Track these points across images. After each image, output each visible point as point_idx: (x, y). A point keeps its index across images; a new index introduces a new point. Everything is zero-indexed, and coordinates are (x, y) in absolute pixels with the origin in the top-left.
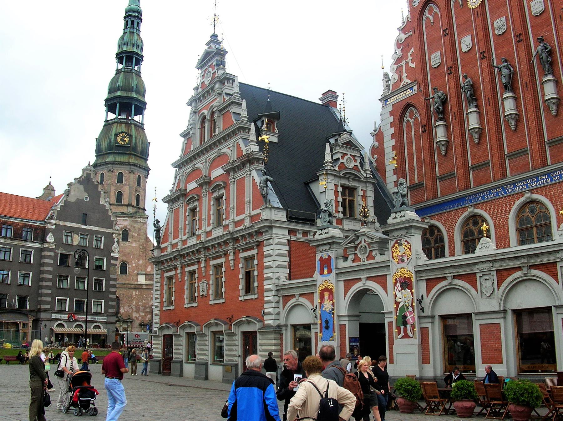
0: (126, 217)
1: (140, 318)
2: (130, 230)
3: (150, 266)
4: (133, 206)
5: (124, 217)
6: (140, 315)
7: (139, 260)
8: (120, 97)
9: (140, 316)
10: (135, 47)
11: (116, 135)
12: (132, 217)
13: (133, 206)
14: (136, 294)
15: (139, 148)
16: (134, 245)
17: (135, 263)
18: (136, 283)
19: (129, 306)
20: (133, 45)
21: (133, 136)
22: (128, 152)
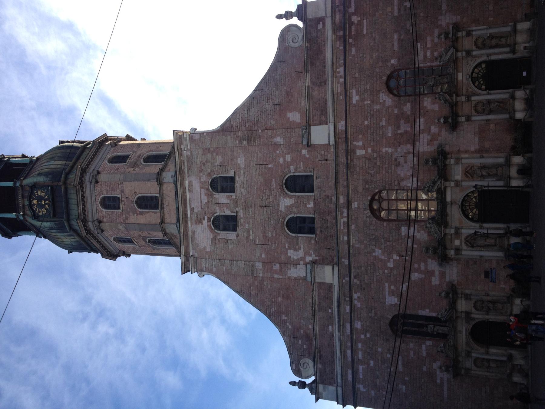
0: (182, 185)
1: (434, 129)
2: (209, 175)
3: (290, 115)
4: (162, 170)
5: (184, 189)
6: (423, 131)
7: (277, 146)
9: (427, 130)
11: (36, 217)
12: (182, 173)
13: (162, 170)
14: (364, 147)
16: (241, 161)
17: (283, 155)
18: (333, 149)
19: (398, 165)
21: (35, 180)
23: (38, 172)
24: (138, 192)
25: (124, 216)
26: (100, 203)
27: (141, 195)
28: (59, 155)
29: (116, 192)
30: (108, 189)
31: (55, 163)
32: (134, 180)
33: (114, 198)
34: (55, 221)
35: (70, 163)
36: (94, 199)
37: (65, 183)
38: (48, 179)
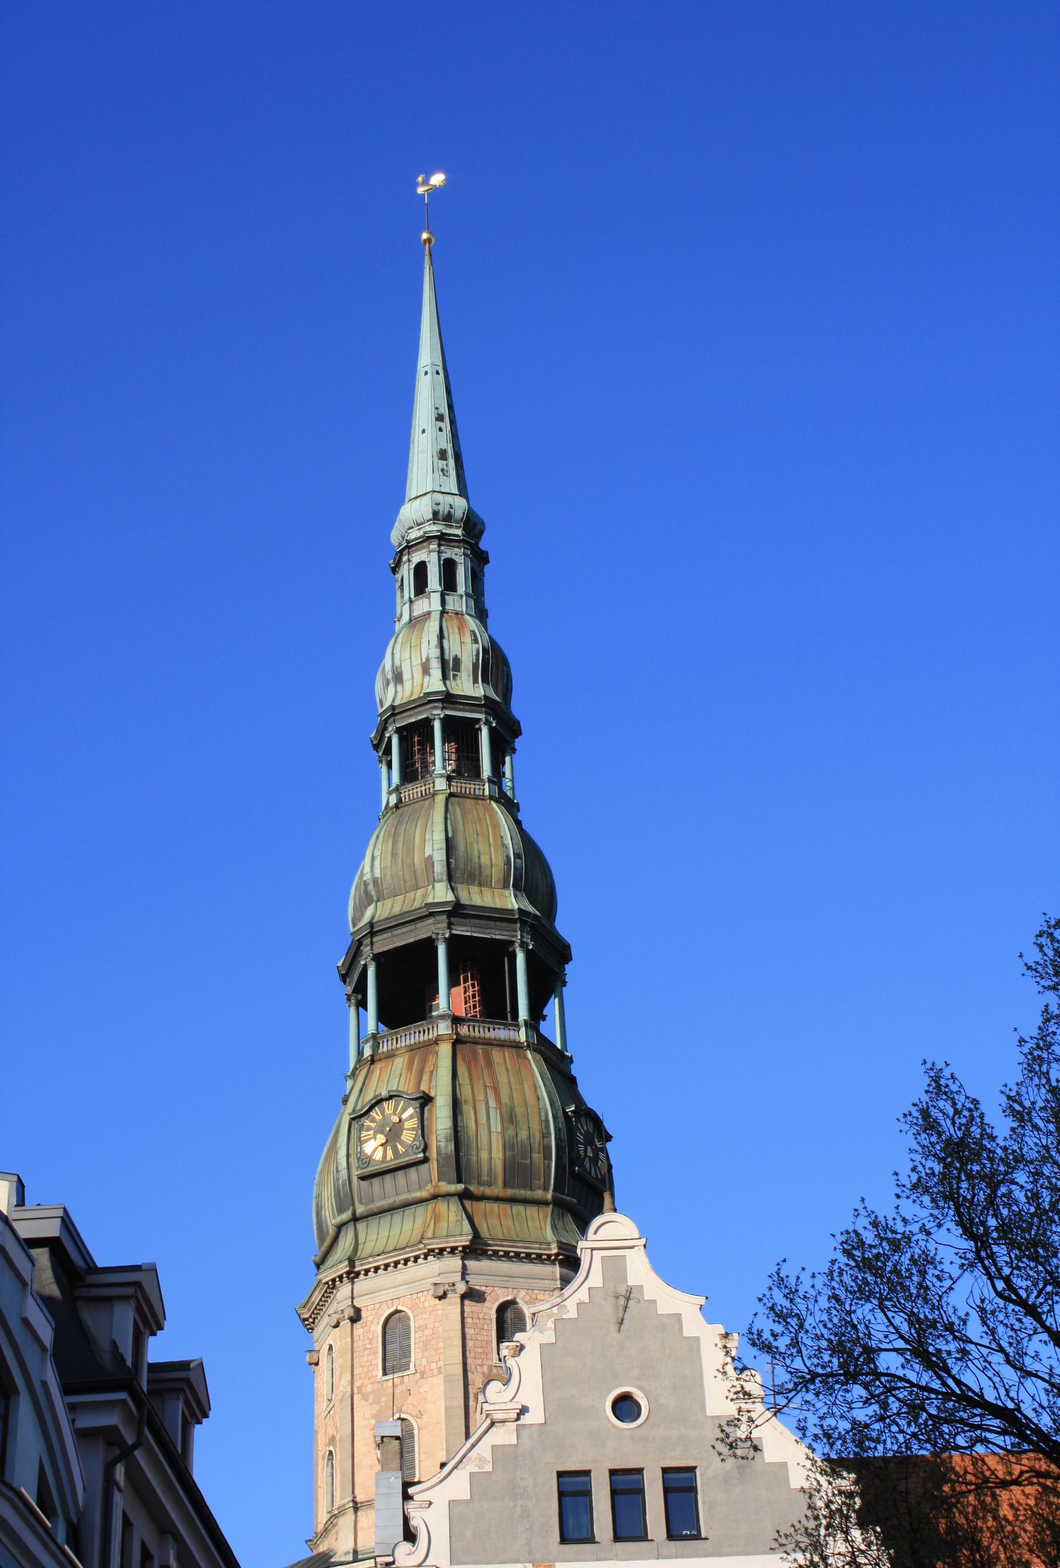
8: (373, 930)
10: (436, 672)
15: (490, 1151)
20: (426, 670)
22: (423, 1194)
23: (465, 1092)
24: (425, 1418)
25: (369, 1388)
26: (397, 1312)
27: (416, 1432)
28: (523, 1134)
29: (420, 1356)
30: (428, 1332)
31: (494, 1137)
32: (447, 1409)
33: (406, 1353)
34: (350, 1183)
35: (497, 1190)
36: (402, 1291)
37: (435, 1197)
38: (442, 1144)
